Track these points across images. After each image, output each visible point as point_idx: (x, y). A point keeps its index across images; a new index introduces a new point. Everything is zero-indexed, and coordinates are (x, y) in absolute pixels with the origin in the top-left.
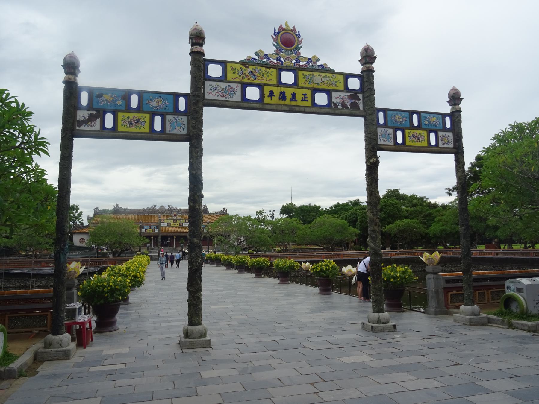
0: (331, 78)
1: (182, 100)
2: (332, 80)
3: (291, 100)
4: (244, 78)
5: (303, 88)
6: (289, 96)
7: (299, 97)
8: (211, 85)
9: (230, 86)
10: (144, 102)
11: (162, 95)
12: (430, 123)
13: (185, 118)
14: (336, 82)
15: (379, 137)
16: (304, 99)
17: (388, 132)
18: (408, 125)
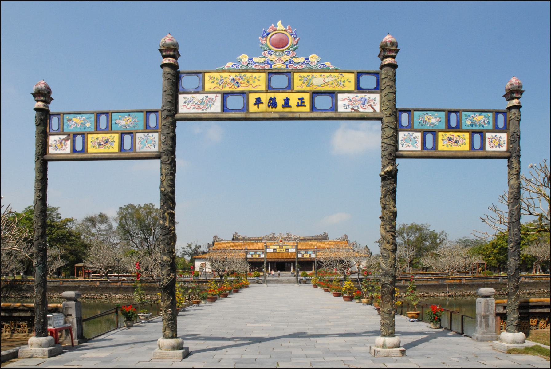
0: (336, 78)
2: (339, 80)
3: (284, 107)
4: (225, 87)
8: (185, 98)
9: (207, 97)
12: (473, 123)
14: (344, 82)
15: (400, 142)
16: (301, 103)
18: (443, 126)
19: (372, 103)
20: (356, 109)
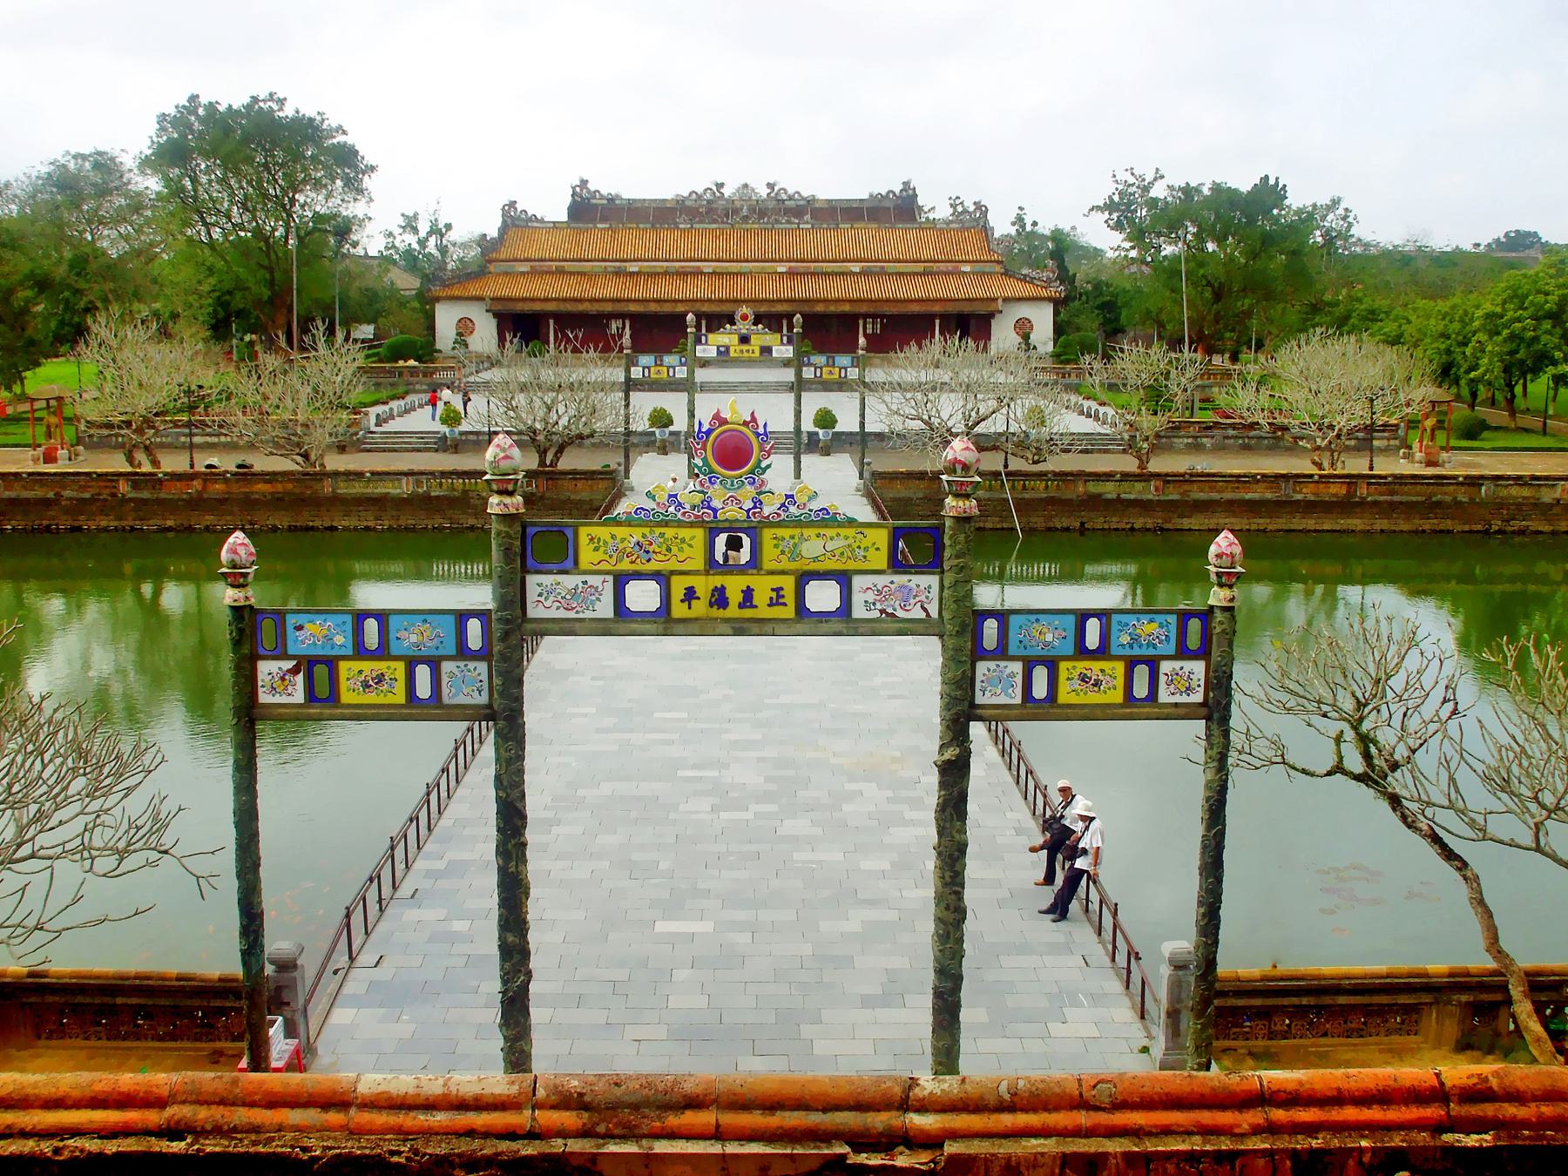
0: (850, 541)
1: (474, 626)
3: (741, 606)
5: (772, 573)
6: (735, 597)
7: (762, 597)
9: (585, 583)
10: (392, 636)
11: (429, 618)
12: (1135, 639)
13: (482, 667)
14: (866, 549)
15: (978, 685)
16: (777, 599)
17: (1008, 671)
19: (923, 598)
20: (890, 610)
